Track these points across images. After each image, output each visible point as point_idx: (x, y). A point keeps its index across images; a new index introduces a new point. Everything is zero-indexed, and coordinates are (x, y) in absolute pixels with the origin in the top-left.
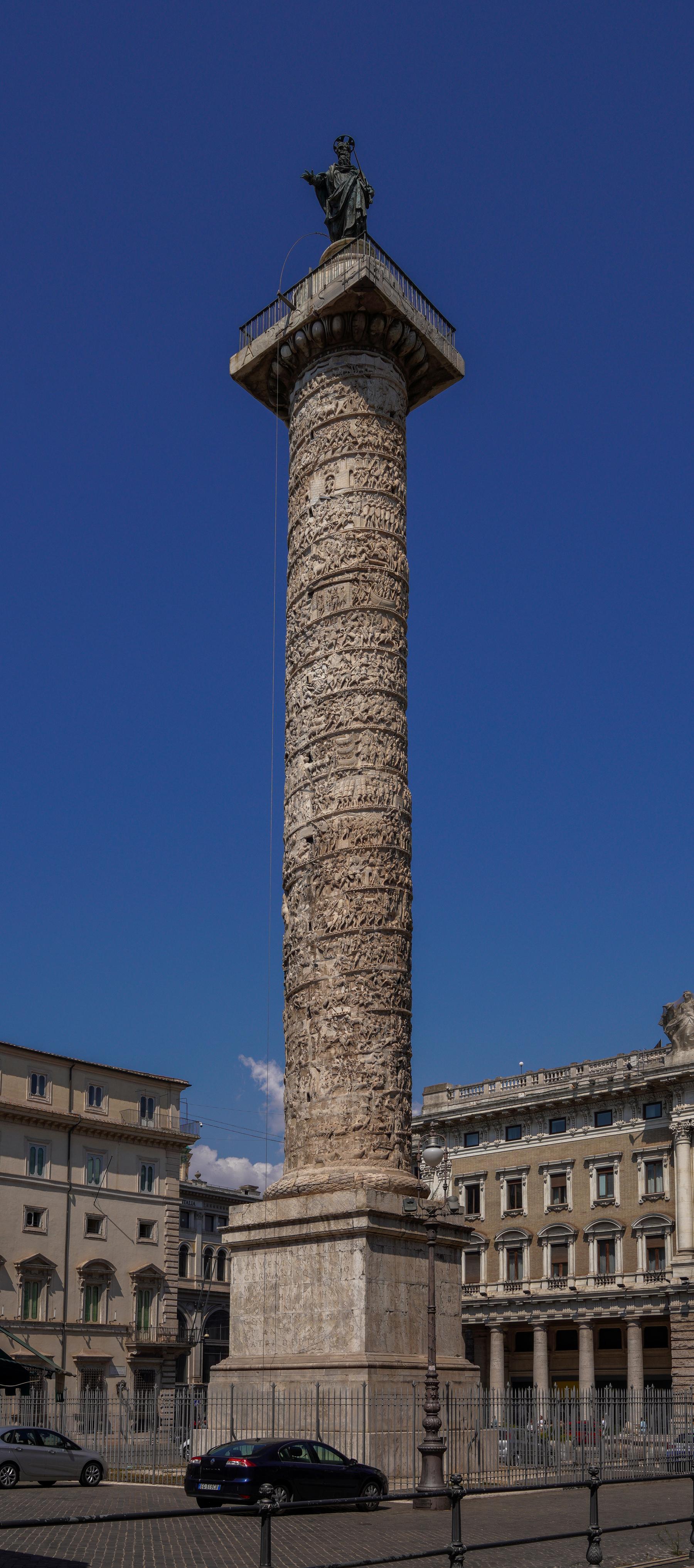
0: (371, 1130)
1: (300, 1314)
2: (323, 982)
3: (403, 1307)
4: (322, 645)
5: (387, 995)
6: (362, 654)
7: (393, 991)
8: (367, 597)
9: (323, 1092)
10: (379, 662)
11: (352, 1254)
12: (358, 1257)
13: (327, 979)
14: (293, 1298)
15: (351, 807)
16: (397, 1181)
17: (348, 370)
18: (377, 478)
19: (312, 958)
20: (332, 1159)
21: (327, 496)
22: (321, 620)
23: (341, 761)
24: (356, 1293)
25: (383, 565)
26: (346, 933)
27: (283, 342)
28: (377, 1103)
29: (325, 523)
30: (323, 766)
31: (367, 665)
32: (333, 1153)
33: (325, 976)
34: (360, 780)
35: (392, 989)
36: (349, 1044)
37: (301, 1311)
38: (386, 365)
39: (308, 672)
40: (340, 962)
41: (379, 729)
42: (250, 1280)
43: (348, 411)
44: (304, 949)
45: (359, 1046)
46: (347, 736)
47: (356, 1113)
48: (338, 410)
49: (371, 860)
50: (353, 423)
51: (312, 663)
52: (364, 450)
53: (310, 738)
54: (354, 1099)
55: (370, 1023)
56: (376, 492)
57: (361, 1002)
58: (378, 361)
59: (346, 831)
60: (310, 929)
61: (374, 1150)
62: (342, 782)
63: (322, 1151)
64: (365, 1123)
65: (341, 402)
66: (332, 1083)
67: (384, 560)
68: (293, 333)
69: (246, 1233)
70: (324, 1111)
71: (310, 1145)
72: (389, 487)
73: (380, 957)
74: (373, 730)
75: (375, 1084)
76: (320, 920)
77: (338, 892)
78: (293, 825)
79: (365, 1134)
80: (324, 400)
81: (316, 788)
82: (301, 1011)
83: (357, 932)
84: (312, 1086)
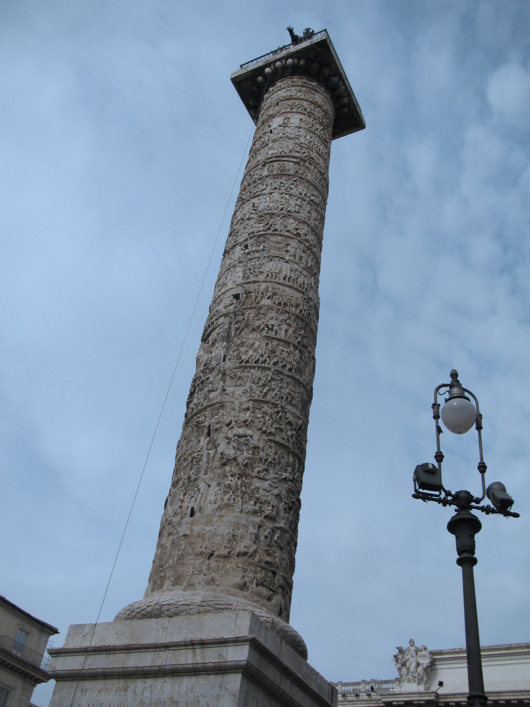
0: (256, 560)
2: (229, 404)
9: (209, 508)
13: (233, 402)
19: (221, 384)
22: (270, 176)
23: (272, 251)
26: (258, 367)
27: (268, 65)
28: (266, 533)
29: (280, 135)
30: (258, 251)
32: (209, 577)
33: (232, 400)
36: (246, 465)
39: (255, 200)
40: (249, 390)
45: (256, 470)
46: (280, 238)
47: (242, 537)
49: (288, 321)
51: (259, 195)
54: (243, 522)
55: (271, 451)
57: (264, 429)
59: (269, 294)
61: (257, 585)
62: (271, 263)
63: (197, 572)
64: (251, 550)
66: (222, 499)
70: (208, 528)
76: (235, 354)
77: (257, 335)
79: (250, 564)
83: (269, 369)
84: (198, 500)
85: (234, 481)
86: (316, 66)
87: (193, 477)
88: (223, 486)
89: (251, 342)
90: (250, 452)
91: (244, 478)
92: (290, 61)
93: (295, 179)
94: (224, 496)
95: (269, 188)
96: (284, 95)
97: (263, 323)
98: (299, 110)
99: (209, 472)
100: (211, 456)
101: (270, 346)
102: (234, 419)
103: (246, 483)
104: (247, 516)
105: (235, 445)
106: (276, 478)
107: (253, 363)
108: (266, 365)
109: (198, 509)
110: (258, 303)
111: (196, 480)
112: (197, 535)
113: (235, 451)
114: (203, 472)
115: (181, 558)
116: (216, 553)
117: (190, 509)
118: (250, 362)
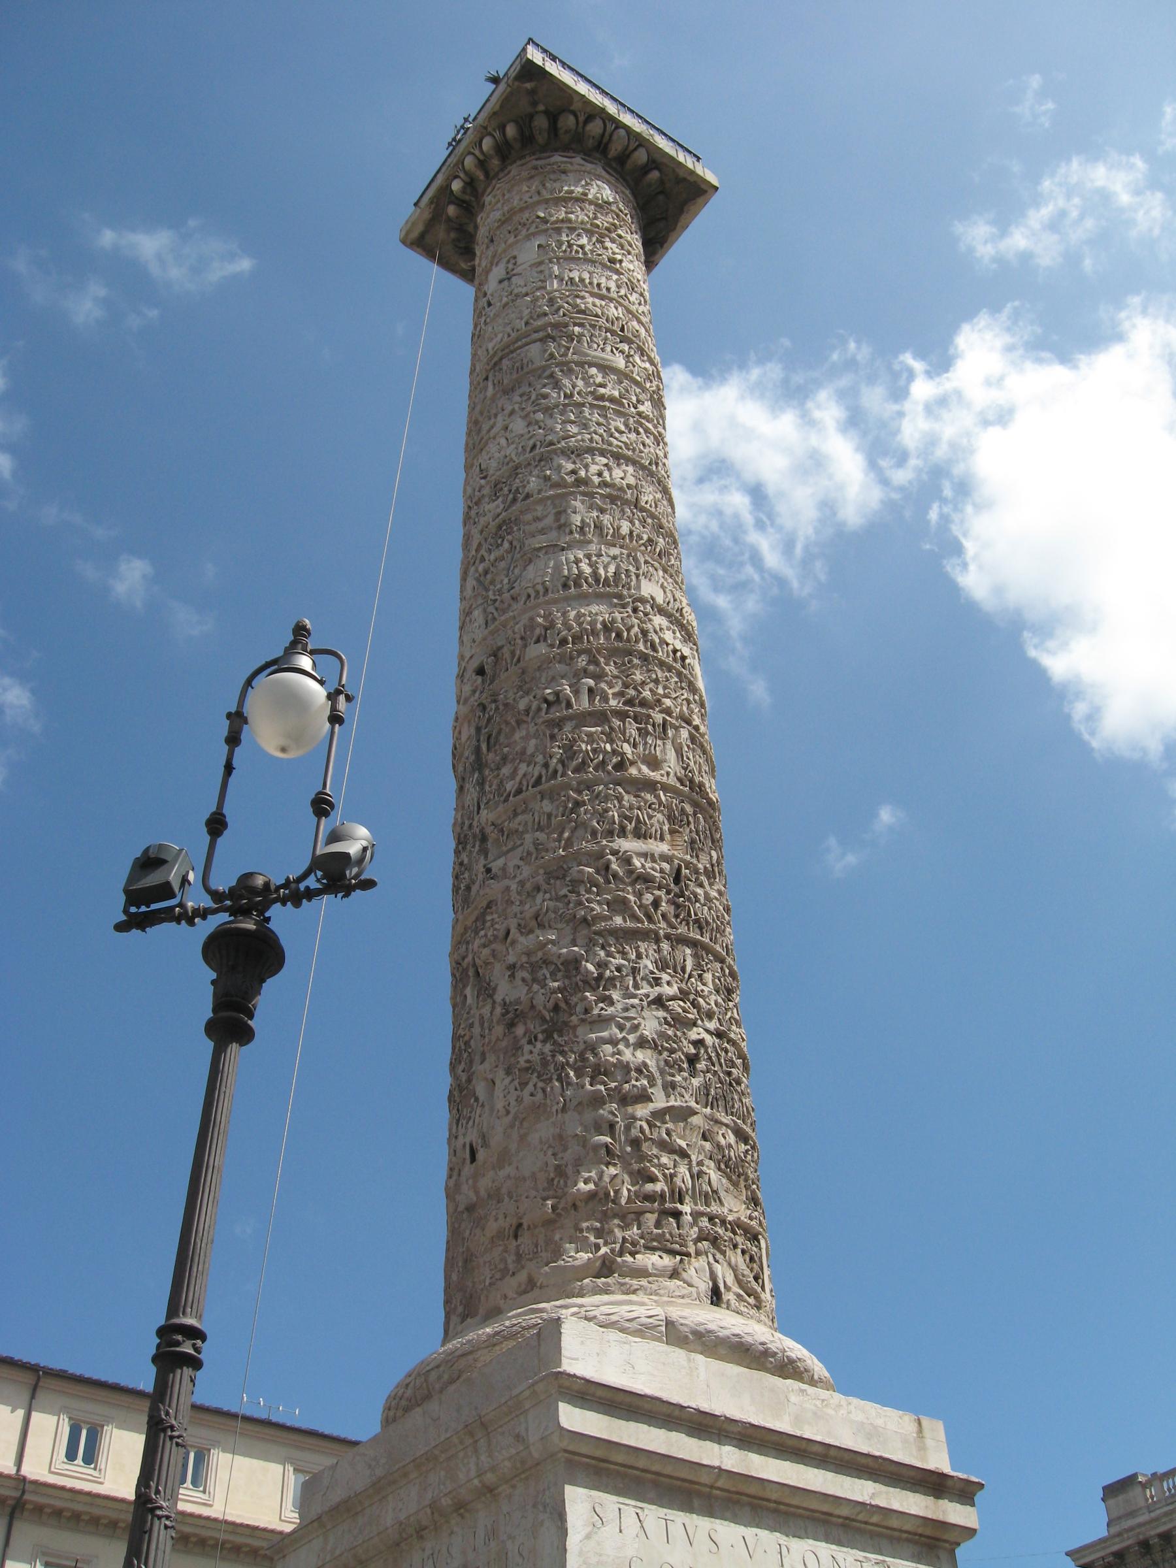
36: (556, 1008)
59: (538, 631)
67: (597, 316)
70: (502, 1173)
86: (541, 122)
88: (516, 1070)
91: (556, 1036)
92: (487, 143)
93: (547, 373)
94: (522, 1091)
95: (500, 418)
97: (534, 697)
98: (532, 230)
103: (563, 1043)
104: (579, 1114)
106: (633, 1006)
107: (530, 788)
109: (480, 1141)
110: (519, 660)
111: (469, 1080)
112: (486, 1196)
113: (527, 988)
114: (477, 1058)
118: (524, 788)
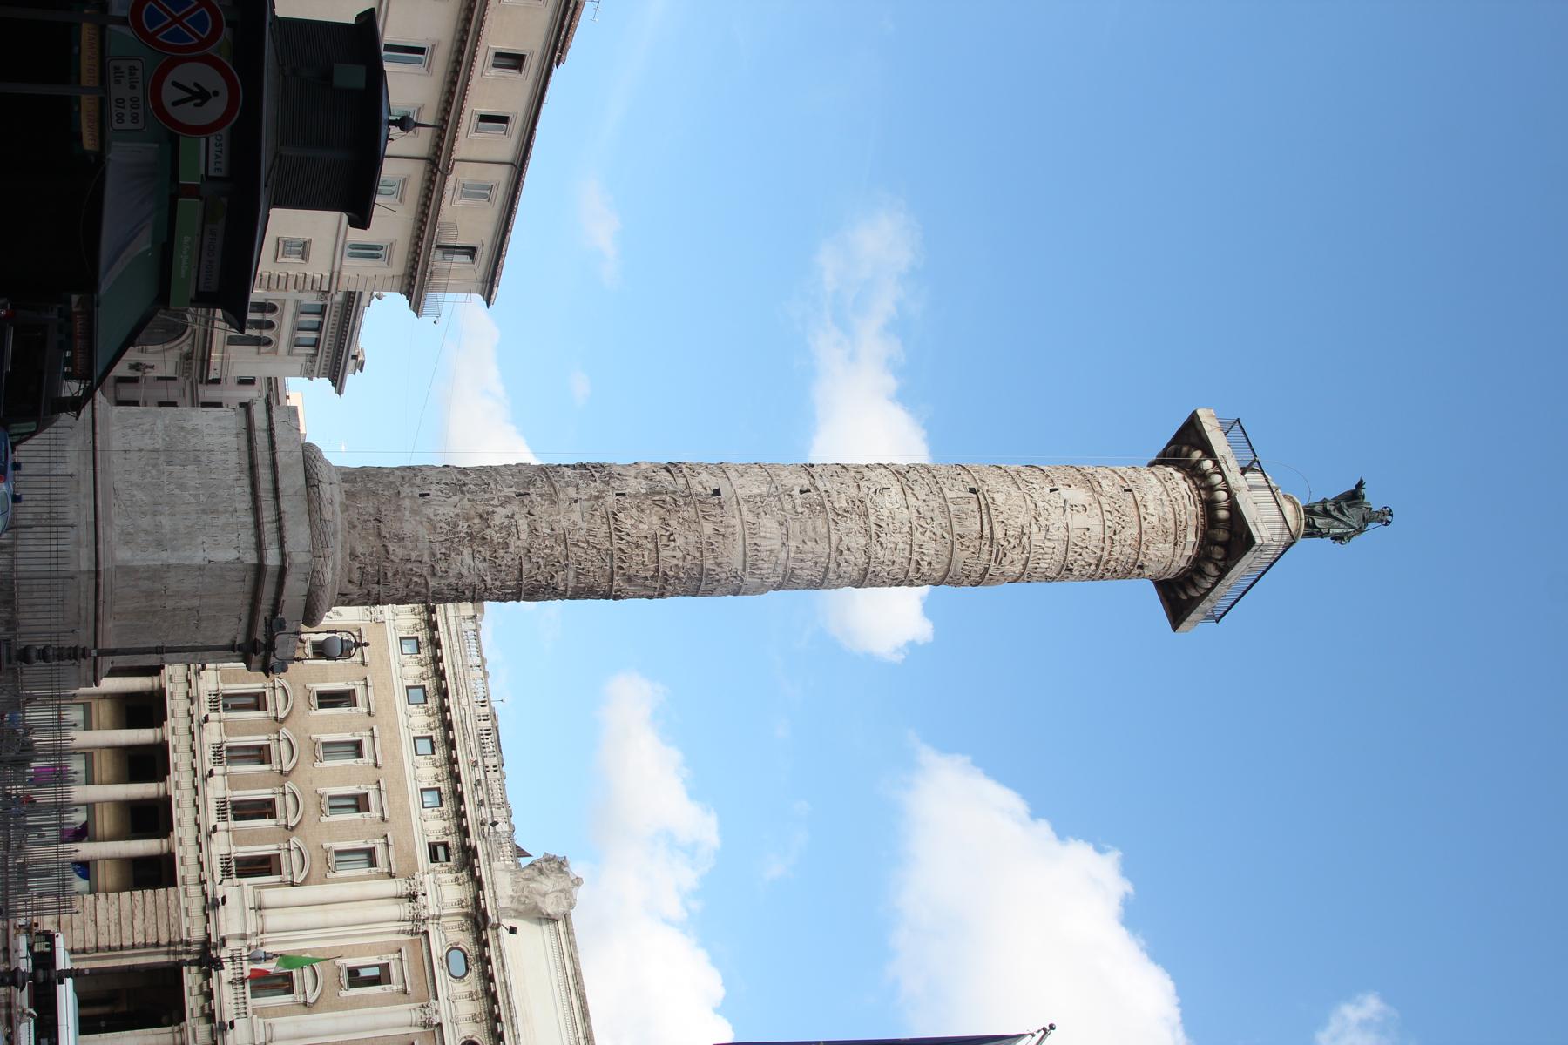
0: (384, 564)
1: (162, 489)
3: (170, 604)
4: (920, 503)
5: (539, 578)
6: (907, 543)
7: (544, 583)
8: (964, 547)
9: (429, 511)
10: (898, 560)
11: (235, 548)
12: (232, 555)
13: (559, 513)
14: (182, 481)
15: (747, 536)
16: (322, 593)
17: (1183, 524)
18: (1080, 555)
20: (349, 523)
21: (1068, 507)
22: (946, 502)
23: (797, 524)
24: (187, 553)
25: (995, 562)
29: (1040, 504)
31: (896, 550)
32: (356, 523)
34: (776, 544)
35: (547, 582)
37: (166, 491)
38: (1185, 561)
39: (896, 488)
41: (829, 562)
42: (206, 431)
43: (1144, 524)
44: (596, 487)
45: (480, 549)
46: (825, 530)
47: (404, 547)
48: (1146, 516)
49: (689, 557)
50: (1135, 531)
52: (1108, 541)
53: (826, 491)
54: (420, 545)
55: (508, 560)
56: (1066, 554)
57: (532, 550)
58: (1188, 552)
59: (722, 530)
60: (617, 494)
63: (360, 511)
64: (392, 557)
65: (1155, 520)
67: (1000, 563)
68: (1222, 473)
69: (265, 425)
70: (407, 513)
71: (368, 497)
72: (1071, 566)
73: (583, 569)
74: (829, 555)
75: (437, 567)
78: (735, 474)
80: (1159, 502)
81: (772, 498)
82: (526, 485)
84: (437, 498)
85: (462, 529)
87: (465, 488)
89: (646, 519)
90: (501, 540)
92: (1222, 495)
93: (946, 535)
96: (1150, 497)
99: (471, 503)
100: (491, 502)
101: (645, 541)
102: (536, 517)
105: (505, 524)
108: (615, 541)
111: (462, 492)
114: (471, 497)
115: (375, 494)
116: (381, 525)
117: (428, 492)
